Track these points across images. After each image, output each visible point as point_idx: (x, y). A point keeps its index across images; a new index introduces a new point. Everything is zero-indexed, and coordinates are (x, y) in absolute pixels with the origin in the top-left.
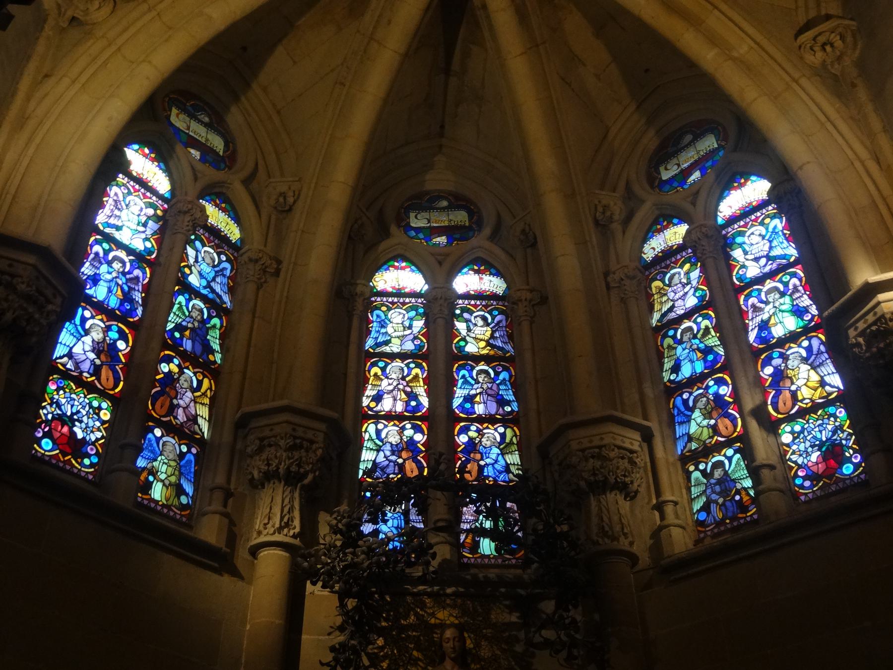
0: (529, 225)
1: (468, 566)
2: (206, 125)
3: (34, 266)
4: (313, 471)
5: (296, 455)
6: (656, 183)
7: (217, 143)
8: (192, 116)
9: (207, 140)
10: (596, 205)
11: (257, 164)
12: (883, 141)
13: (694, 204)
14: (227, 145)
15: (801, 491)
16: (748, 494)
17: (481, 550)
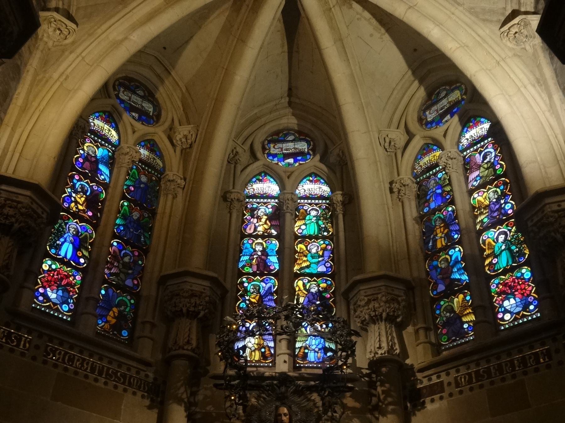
0: (343, 152)
1: (300, 368)
2: (141, 97)
3: (30, 197)
4: (202, 310)
5: (193, 301)
6: (424, 122)
7: (148, 107)
8: (134, 92)
9: (143, 107)
10: (385, 138)
11: (173, 120)
12: (557, 96)
13: (445, 136)
14: (154, 110)
15: (501, 322)
16: (269, 350)
17: (308, 359)
